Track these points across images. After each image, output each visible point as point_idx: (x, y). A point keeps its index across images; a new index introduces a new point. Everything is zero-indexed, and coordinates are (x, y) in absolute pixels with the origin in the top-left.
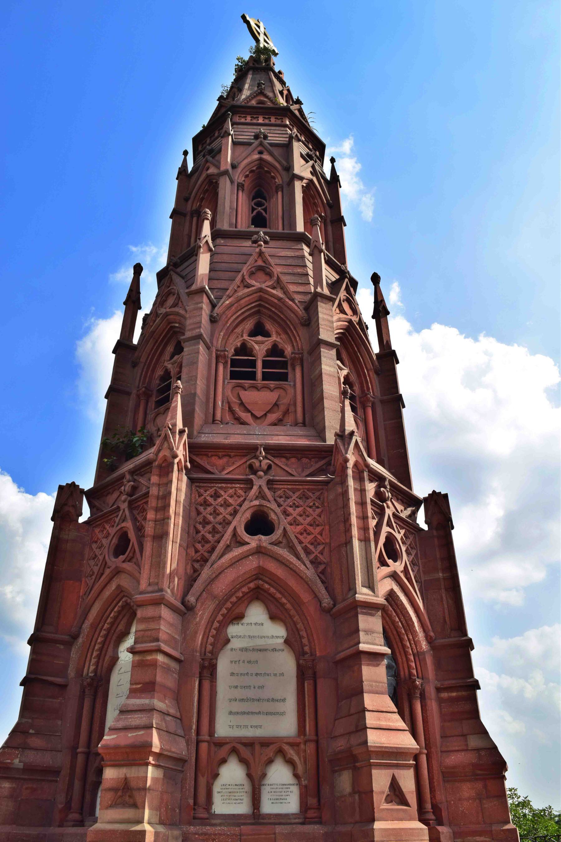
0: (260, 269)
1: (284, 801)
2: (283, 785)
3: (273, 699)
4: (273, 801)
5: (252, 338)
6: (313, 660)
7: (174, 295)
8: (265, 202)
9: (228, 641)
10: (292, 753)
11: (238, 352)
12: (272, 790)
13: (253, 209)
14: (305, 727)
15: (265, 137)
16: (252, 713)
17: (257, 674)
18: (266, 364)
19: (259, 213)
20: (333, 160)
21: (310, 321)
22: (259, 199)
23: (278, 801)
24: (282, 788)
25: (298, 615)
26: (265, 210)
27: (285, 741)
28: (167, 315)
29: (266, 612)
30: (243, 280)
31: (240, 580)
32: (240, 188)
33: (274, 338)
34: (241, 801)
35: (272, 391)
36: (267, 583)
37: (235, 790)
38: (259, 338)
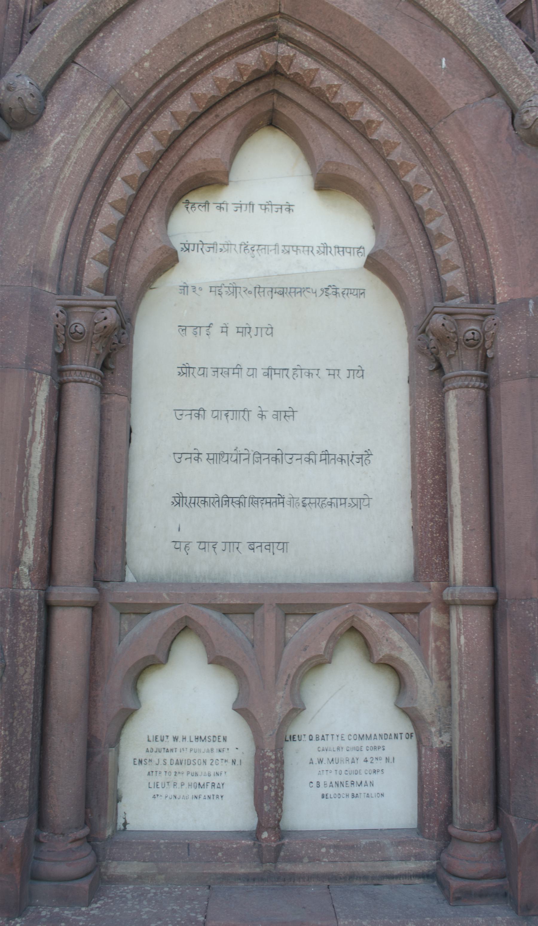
1: (363, 790)
2: (361, 737)
3: (326, 454)
4: (323, 790)
6: (485, 316)
9: (169, 260)
10: (394, 640)
12: (325, 755)
14: (445, 552)
16: (255, 501)
17: (270, 372)
23: (343, 790)
24: (359, 749)
25: (425, 160)
27: (372, 599)
29: (303, 167)
31: (210, 31)
34: (216, 791)
36: (308, 51)
37: (197, 756)
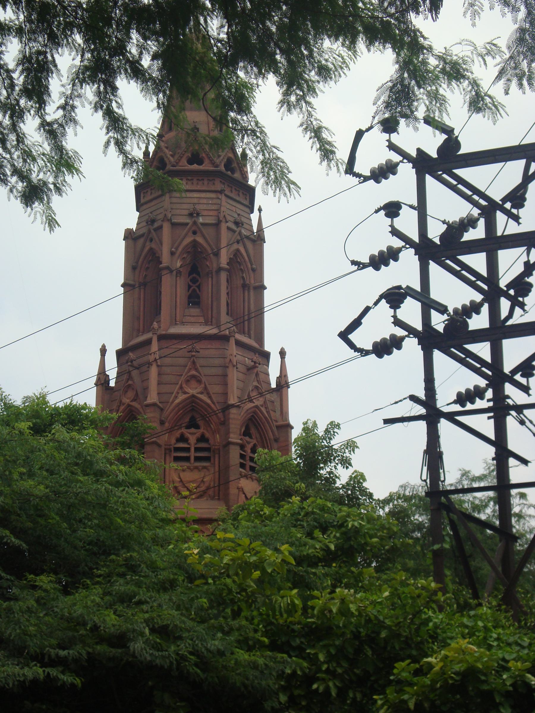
0: (193, 376)
5: (188, 430)
7: (133, 389)
8: (198, 277)
11: (178, 440)
13: (190, 287)
15: (198, 214)
18: (197, 450)
19: (194, 290)
20: (260, 210)
21: (224, 423)
22: (194, 275)
26: (199, 287)
28: (129, 405)
30: (181, 388)
32: (178, 275)
33: (201, 430)
35: (200, 471)
38: (193, 430)
